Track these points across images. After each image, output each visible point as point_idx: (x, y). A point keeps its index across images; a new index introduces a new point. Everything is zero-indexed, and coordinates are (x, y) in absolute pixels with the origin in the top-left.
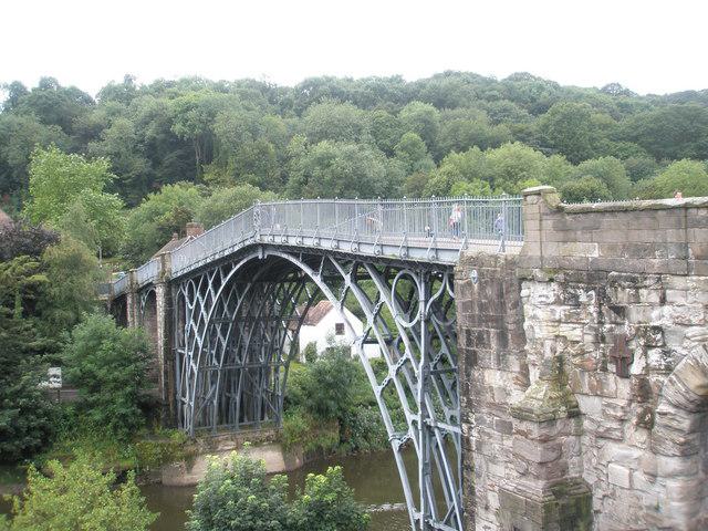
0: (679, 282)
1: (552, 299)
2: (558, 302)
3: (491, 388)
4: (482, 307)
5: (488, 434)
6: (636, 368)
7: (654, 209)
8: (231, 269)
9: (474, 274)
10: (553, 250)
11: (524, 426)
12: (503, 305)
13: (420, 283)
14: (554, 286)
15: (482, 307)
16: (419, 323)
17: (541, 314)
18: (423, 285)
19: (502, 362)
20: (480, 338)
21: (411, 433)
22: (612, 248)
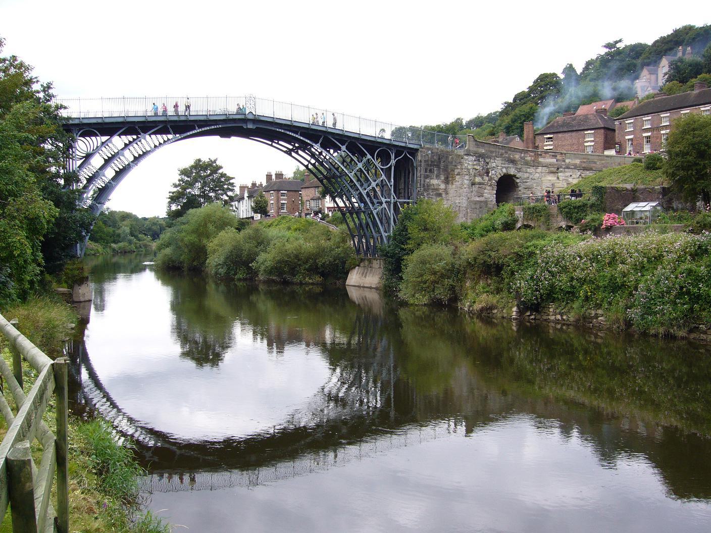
0: (497, 159)
1: (474, 160)
2: (475, 161)
3: (433, 185)
4: (432, 162)
5: (432, 198)
6: (490, 175)
7: (494, 145)
8: (195, 129)
9: (430, 152)
10: (475, 149)
11: (481, 186)
12: (440, 162)
13: (392, 153)
14: (475, 157)
15: (432, 162)
16: (391, 166)
17: (470, 163)
18: (394, 154)
19: (438, 177)
20: (430, 171)
21: (384, 205)
22: (486, 151)
